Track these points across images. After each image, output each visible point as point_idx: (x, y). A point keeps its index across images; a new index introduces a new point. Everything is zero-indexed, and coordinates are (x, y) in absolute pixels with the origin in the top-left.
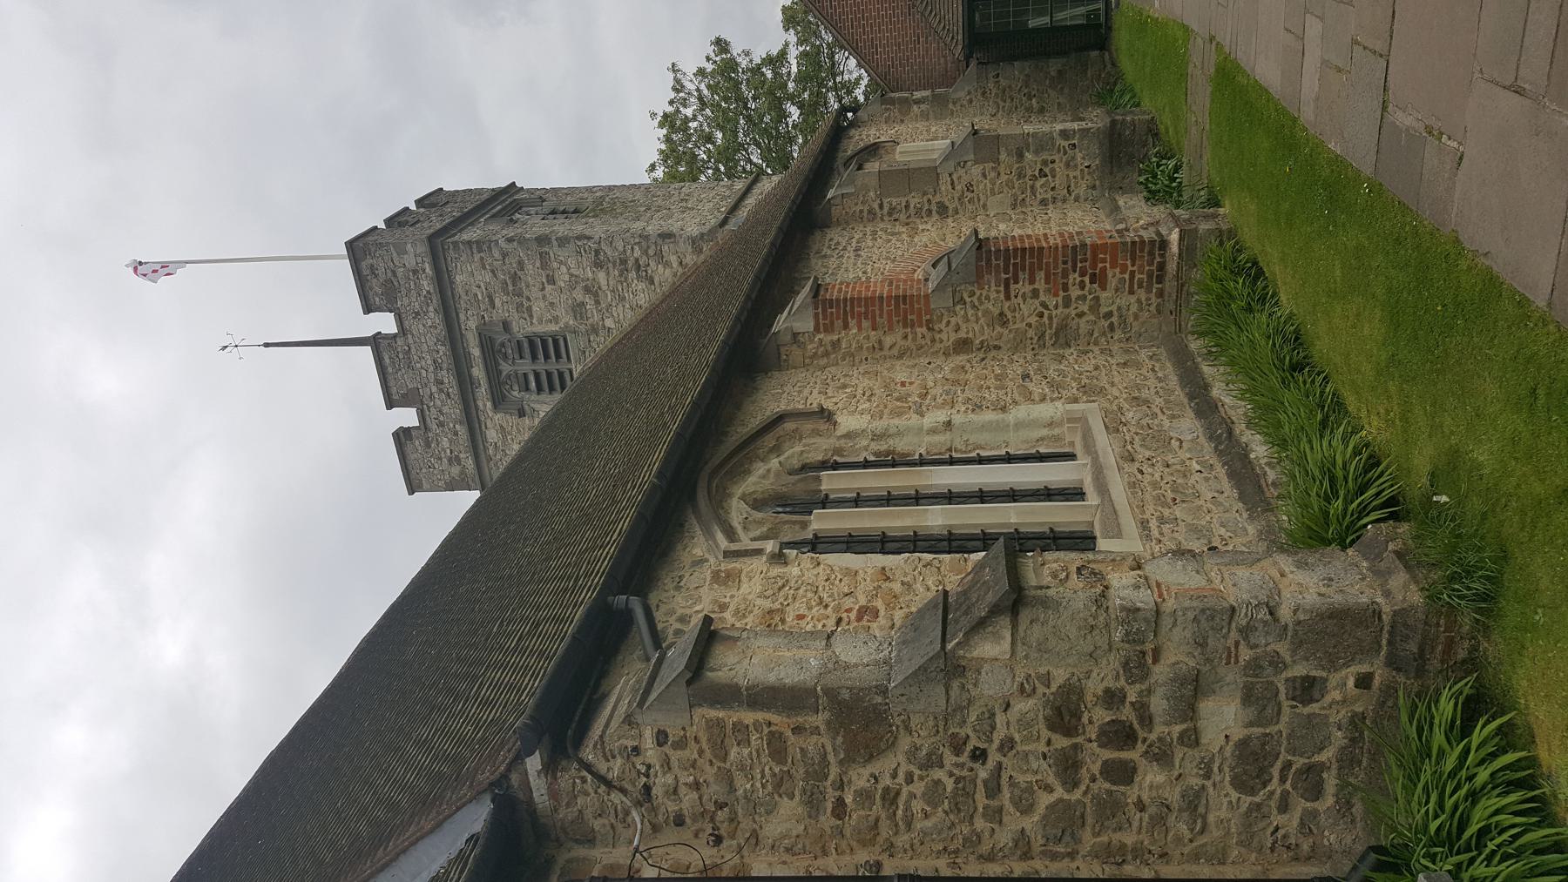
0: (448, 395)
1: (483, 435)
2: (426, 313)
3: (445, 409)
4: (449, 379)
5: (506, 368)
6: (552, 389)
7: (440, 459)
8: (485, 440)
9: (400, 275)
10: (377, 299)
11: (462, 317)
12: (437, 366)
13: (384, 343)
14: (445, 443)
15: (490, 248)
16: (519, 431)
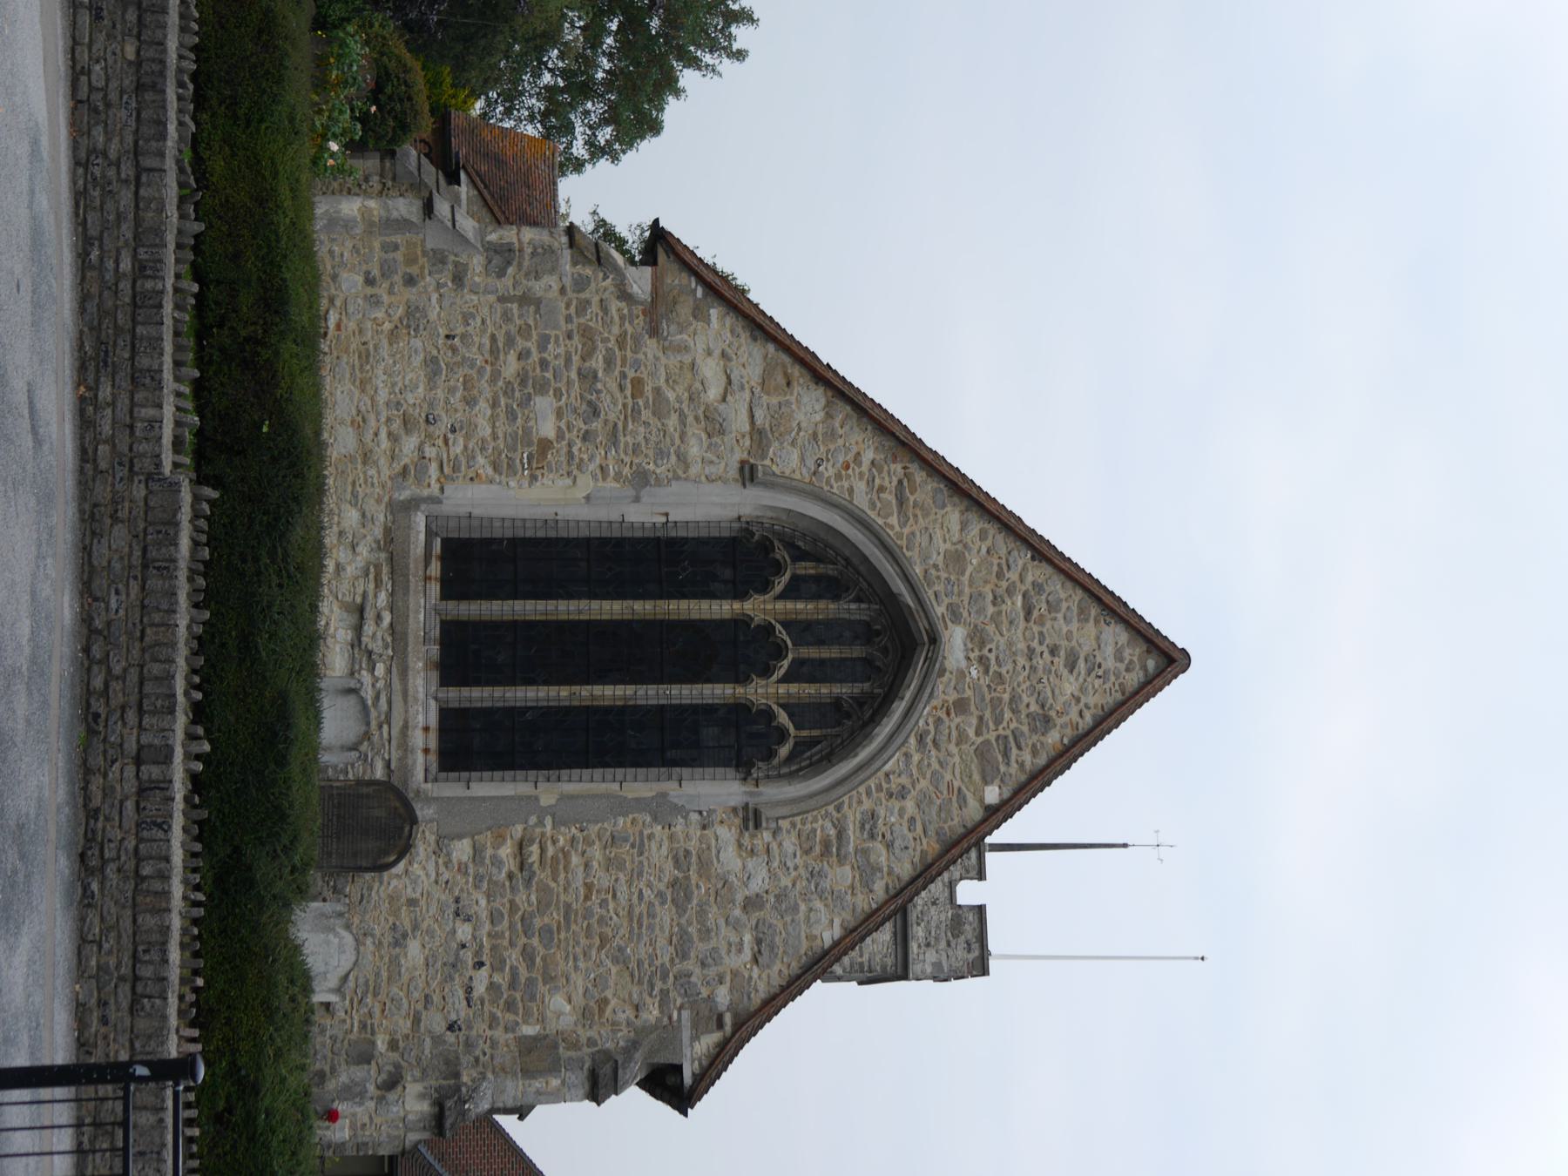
2: (925, 904)
9: (943, 944)
10: (971, 918)
13: (973, 873)
15: (852, 965)
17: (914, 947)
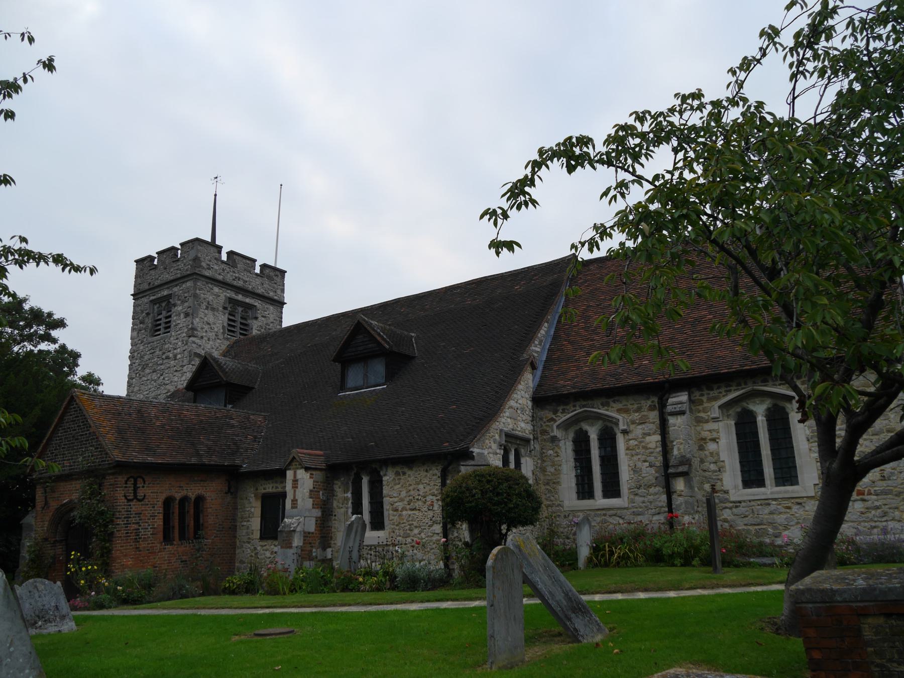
0: (234, 280)
1: (218, 286)
3: (229, 275)
4: (240, 283)
5: (240, 309)
6: (229, 325)
7: (210, 261)
8: (215, 285)
9: (275, 286)
11: (260, 302)
12: (245, 282)
14: (216, 267)
16: (218, 303)
17: (276, 298)
